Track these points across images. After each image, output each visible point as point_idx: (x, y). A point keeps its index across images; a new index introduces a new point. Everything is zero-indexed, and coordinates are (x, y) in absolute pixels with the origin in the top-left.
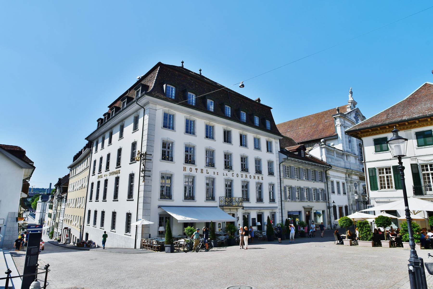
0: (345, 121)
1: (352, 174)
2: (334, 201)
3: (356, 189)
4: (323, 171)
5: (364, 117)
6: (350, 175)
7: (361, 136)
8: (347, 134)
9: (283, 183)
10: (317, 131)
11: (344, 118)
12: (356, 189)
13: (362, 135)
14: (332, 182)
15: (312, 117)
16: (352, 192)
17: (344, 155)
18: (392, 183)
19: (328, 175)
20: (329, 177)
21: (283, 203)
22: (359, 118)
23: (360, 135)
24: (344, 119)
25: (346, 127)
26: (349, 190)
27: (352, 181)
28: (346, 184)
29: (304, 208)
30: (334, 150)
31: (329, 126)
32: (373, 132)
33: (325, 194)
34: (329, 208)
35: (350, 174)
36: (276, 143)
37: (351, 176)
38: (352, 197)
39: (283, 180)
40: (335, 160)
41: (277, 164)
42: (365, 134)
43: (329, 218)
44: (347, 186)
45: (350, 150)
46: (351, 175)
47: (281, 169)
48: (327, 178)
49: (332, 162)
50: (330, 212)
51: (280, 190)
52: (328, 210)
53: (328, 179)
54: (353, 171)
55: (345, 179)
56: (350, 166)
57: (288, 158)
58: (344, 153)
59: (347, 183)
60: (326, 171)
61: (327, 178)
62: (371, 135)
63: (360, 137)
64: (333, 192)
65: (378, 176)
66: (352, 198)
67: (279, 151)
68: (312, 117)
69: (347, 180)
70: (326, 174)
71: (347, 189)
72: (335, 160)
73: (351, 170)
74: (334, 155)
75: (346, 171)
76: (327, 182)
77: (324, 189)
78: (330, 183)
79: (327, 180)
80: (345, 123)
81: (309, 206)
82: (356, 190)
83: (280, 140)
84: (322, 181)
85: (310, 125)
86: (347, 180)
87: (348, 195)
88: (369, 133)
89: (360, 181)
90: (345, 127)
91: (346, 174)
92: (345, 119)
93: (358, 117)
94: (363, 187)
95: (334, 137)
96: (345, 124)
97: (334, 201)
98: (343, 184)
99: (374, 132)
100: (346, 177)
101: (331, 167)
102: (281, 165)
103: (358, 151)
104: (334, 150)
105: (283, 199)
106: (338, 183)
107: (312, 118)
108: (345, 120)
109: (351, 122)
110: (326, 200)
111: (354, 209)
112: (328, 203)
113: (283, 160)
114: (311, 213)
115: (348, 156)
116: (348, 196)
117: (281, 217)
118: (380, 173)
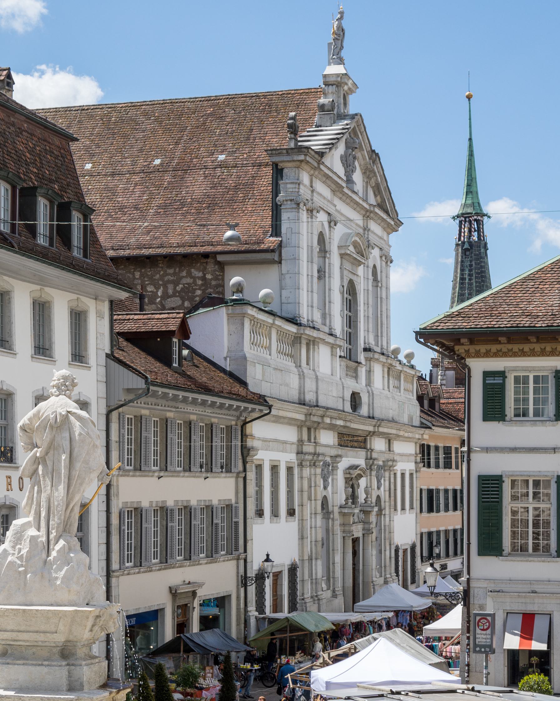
0: (314, 185)
1: (321, 425)
2: (268, 555)
3: (325, 488)
4: (233, 423)
5: (377, 155)
6: (312, 430)
7: (467, 351)
8: (422, 340)
9: (117, 495)
10: (183, 205)
11: (315, 169)
12: (325, 488)
13: (472, 349)
14: (259, 467)
15: (146, 114)
16: (313, 502)
17: (300, 343)
18: (547, 536)
19: (250, 443)
20: (253, 448)
21: (114, 581)
22: (356, 163)
23: (466, 348)
24: (312, 172)
25: (315, 212)
26: (305, 495)
27: (319, 455)
28: (296, 471)
29: (174, 592)
30: (273, 324)
31: (236, 188)
32: (510, 346)
33: (237, 523)
34: (244, 581)
35: (315, 425)
36: (100, 315)
37: (317, 431)
38: (313, 526)
39: (117, 481)
40: (275, 369)
41: (98, 413)
42: (483, 348)
43: (243, 626)
44: (302, 478)
45: (317, 317)
46: (315, 429)
47: (114, 437)
48: (246, 451)
49: (263, 382)
50: (248, 600)
51: (105, 525)
52: (242, 590)
53: (248, 459)
54: (328, 413)
55: (294, 447)
56: (317, 393)
57: (148, 389)
58: (302, 334)
59: (301, 465)
60: (245, 423)
61: (245, 453)
62: (501, 354)
63: (463, 355)
64: (260, 513)
65: (508, 505)
66: (313, 529)
67: (106, 354)
68: (146, 114)
69: (302, 453)
70: (244, 436)
71: (301, 491)
72: (275, 369)
73: (320, 412)
74: (269, 348)
75: (302, 417)
76: (245, 470)
77: (233, 501)
78: (251, 475)
79: (245, 463)
80: (315, 194)
81: (189, 583)
82: (324, 493)
83: (111, 302)
84: (229, 471)
85: (141, 162)
86: (302, 453)
87: (302, 516)
88: (499, 347)
89: (340, 451)
90: (312, 211)
91: (300, 427)
92: (317, 173)
93: (355, 158)
94: (348, 476)
95: (268, 256)
96: (316, 198)
97: (268, 555)
98: (290, 470)
99: (516, 347)
100: (301, 442)
101: (270, 407)
102: (115, 415)
103: (343, 318)
104: (273, 324)
105: (115, 566)
106: (274, 469)
107: (148, 125)
108: (314, 179)
109: (334, 186)
110: (237, 549)
111: (316, 574)
112: (242, 562)
113: (123, 397)
114: (191, 609)
115: (314, 345)
116: (302, 520)
117: (104, 644)
118: (514, 498)
